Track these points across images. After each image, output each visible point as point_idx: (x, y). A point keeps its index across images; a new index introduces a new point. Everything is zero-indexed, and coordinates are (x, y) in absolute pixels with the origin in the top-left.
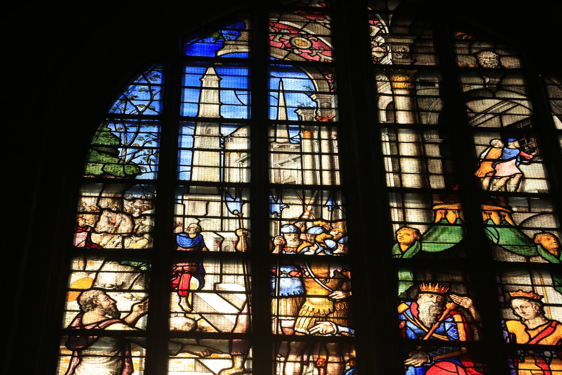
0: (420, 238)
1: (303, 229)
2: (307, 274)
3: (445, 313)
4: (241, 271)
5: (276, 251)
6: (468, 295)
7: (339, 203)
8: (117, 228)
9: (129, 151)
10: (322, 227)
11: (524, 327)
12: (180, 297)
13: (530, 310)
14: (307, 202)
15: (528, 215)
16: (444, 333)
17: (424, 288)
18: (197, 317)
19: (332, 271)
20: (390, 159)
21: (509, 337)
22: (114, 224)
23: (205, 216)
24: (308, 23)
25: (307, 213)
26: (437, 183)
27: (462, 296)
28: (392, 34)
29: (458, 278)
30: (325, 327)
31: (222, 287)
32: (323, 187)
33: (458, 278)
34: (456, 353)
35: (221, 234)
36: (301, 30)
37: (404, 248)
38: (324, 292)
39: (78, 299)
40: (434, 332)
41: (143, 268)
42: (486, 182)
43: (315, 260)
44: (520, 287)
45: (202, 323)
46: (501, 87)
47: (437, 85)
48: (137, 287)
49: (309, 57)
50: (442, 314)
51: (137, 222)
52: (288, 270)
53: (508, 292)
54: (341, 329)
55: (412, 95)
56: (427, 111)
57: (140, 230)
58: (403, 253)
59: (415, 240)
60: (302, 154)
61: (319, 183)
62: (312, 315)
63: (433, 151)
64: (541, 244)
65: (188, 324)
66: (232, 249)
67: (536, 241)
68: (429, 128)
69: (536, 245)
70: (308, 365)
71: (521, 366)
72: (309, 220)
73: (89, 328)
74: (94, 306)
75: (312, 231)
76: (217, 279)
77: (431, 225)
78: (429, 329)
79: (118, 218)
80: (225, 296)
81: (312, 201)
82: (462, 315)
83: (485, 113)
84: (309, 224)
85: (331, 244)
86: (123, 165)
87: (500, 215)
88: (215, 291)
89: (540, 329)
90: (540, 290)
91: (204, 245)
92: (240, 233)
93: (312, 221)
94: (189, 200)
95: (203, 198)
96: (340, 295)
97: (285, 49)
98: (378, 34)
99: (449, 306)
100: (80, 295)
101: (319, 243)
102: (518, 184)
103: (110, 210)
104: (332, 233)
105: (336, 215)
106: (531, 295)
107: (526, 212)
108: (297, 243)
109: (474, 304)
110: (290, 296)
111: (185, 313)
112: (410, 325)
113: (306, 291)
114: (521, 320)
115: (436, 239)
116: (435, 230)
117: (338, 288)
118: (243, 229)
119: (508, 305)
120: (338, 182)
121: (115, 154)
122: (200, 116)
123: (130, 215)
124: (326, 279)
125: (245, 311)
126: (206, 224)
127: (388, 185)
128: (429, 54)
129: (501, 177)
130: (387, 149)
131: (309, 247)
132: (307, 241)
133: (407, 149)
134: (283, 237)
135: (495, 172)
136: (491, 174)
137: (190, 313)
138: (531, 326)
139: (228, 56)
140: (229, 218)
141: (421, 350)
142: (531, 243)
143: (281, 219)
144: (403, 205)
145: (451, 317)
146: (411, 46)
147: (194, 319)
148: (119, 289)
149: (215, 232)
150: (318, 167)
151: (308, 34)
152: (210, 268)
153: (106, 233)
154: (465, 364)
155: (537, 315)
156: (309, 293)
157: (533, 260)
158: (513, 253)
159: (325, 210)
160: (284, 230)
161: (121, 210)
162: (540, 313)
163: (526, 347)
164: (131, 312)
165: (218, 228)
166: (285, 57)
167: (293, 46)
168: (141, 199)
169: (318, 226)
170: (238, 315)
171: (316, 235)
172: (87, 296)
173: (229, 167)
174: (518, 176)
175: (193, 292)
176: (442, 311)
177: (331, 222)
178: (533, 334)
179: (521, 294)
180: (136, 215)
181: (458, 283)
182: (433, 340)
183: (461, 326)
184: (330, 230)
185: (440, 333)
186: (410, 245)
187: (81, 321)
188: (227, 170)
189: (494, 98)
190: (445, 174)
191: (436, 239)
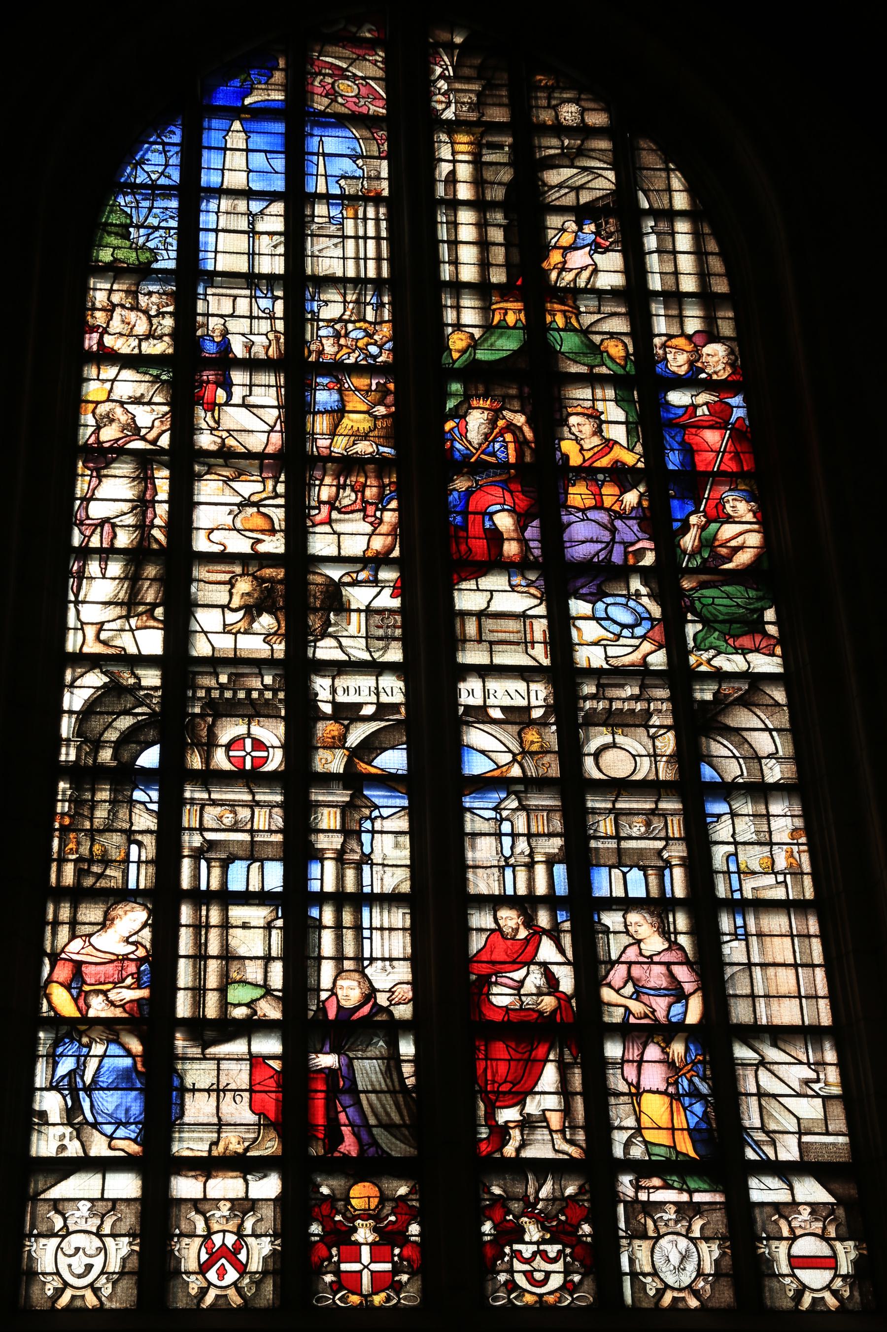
0: (474, 344)
1: (343, 332)
2: (346, 386)
3: (497, 430)
4: (273, 383)
5: (313, 358)
6: (522, 411)
7: (386, 299)
8: (132, 329)
9: (142, 231)
10: (365, 330)
11: (578, 447)
12: (206, 411)
13: (587, 427)
14: (349, 298)
15: (597, 317)
16: (493, 454)
17: (474, 403)
18: (225, 434)
19: (374, 382)
20: (446, 245)
21: (561, 458)
22: (129, 324)
23: (232, 316)
24: (355, 60)
25: (348, 313)
26: (498, 276)
27: (516, 412)
28: (457, 78)
29: (513, 392)
30: (364, 448)
31: (251, 400)
32: (367, 281)
33: (513, 392)
34: (504, 477)
35: (252, 337)
36: (346, 70)
37: (455, 355)
38: (364, 408)
39: (93, 412)
40: (482, 453)
41: (164, 377)
42: (554, 275)
43: (356, 369)
44: (581, 402)
45: (230, 442)
46: (582, 152)
47: (507, 149)
48: (157, 399)
49: (356, 109)
50: (492, 433)
51: (155, 321)
52: (325, 381)
53: (566, 407)
54: (382, 449)
55: (477, 163)
56: (493, 183)
57: (159, 332)
58: (454, 362)
59: (469, 346)
60: (344, 237)
61: (363, 275)
62: (350, 433)
63: (497, 235)
64: (607, 352)
65: (215, 443)
66: (262, 356)
67: (602, 348)
68: (494, 205)
69: (601, 353)
70: (344, 489)
71: (571, 490)
72: (350, 321)
73: (107, 445)
74: (112, 421)
75: (353, 335)
76: (246, 391)
77: (488, 328)
78: (477, 450)
79: (132, 316)
80: (255, 410)
81: (354, 297)
82: (514, 434)
83: (560, 186)
84: (350, 327)
85: (373, 350)
86: (136, 249)
87: (566, 317)
88: (244, 405)
89: (596, 450)
90: (600, 406)
91: (231, 351)
92: (271, 336)
93: (354, 322)
94: (213, 295)
95: (229, 291)
96: (381, 410)
97: (326, 96)
98: (442, 76)
99: (501, 423)
100: (95, 408)
101: (361, 349)
102: (589, 279)
103: (123, 306)
104: (376, 337)
105: (382, 316)
106: (590, 411)
107: (594, 313)
108: (336, 349)
109: (528, 422)
110: (326, 412)
111: (212, 429)
112: (458, 445)
113: (344, 406)
114: (577, 440)
115: (492, 345)
116: (492, 334)
117: (381, 402)
118: (276, 331)
119: (564, 422)
120: (385, 274)
121: (126, 236)
122: (224, 187)
123: (146, 312)
124: (367, 391)
125: (278, 428)
126: (234, 325)
127: (443, 278)
128: (500, 105)
129: (572, 270)
130: (443, 233)
131: (349, 353)
132: (347, 347)
133: (467, 233)
134: (321, 342)
135: (565, 262)
136: (559, 266)
137: (217, 429)
138: (586, 447)
139: (258, 105)
140: (259, 318)
141: (467, 473)
142: (596, 350)
143: (319, 320)
144: (458, 302)
145: (502, 436)
146: (479, 94)
147: (221, 437)
148: (137, 401)
149: (243, 335)
150: (362, 255)
151: (355, 75)
152: (238, 377)
153: (121, 334)
154: (513, 487)
155: (594, 434)
156: (347, 409)
157: (596, 370)
158: (576, 362)
159: (369, 309)
160: (322, 332)
161: (135, 308)
162: (598, 432)
163: (579, 469)
164: (152, 428)
165: (247, 331)
166: (327, 107)
167: (336, 92)
168: (158, 292)
169: (360, 328)
170: (269, 432)
171: (357, 340)
172: (102, 409)
173: (259, 254)
174: (591, 268)
175: (220, 405)
176: (493, 429)
177: (375, 323)
178: (588, 455)
179: (579, 410)
180: (153, 313)
181: (512, 397)
182: (481, 463)
183: (511, 446)
184: (374, 334)
185: (489, 455)
186: (463, 352)
187: (98, 438)
188: (257, 257)
189: (572, 166)
190: (508, 265)
191: (492, 345)
